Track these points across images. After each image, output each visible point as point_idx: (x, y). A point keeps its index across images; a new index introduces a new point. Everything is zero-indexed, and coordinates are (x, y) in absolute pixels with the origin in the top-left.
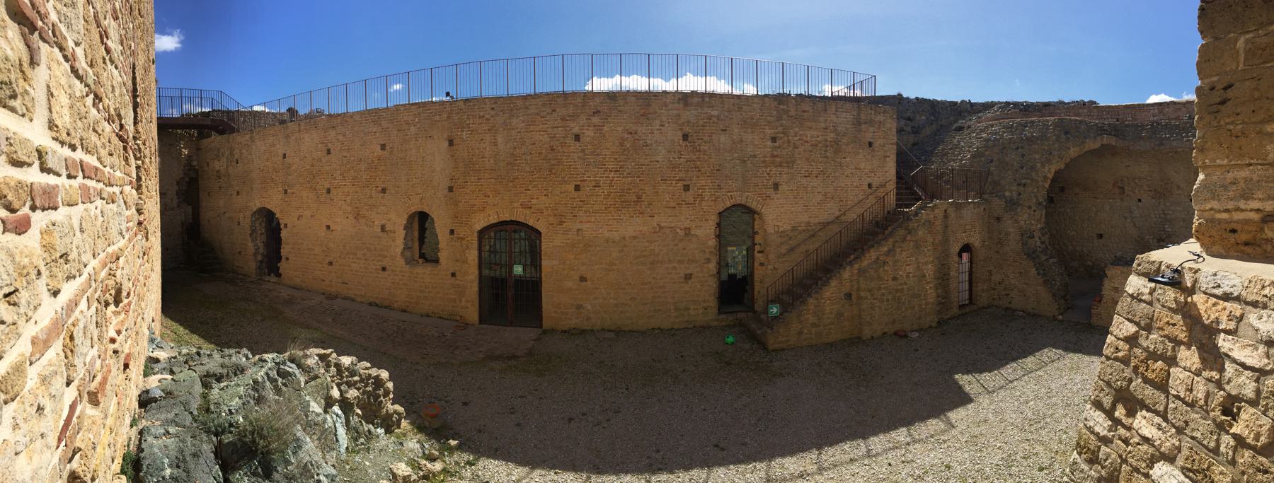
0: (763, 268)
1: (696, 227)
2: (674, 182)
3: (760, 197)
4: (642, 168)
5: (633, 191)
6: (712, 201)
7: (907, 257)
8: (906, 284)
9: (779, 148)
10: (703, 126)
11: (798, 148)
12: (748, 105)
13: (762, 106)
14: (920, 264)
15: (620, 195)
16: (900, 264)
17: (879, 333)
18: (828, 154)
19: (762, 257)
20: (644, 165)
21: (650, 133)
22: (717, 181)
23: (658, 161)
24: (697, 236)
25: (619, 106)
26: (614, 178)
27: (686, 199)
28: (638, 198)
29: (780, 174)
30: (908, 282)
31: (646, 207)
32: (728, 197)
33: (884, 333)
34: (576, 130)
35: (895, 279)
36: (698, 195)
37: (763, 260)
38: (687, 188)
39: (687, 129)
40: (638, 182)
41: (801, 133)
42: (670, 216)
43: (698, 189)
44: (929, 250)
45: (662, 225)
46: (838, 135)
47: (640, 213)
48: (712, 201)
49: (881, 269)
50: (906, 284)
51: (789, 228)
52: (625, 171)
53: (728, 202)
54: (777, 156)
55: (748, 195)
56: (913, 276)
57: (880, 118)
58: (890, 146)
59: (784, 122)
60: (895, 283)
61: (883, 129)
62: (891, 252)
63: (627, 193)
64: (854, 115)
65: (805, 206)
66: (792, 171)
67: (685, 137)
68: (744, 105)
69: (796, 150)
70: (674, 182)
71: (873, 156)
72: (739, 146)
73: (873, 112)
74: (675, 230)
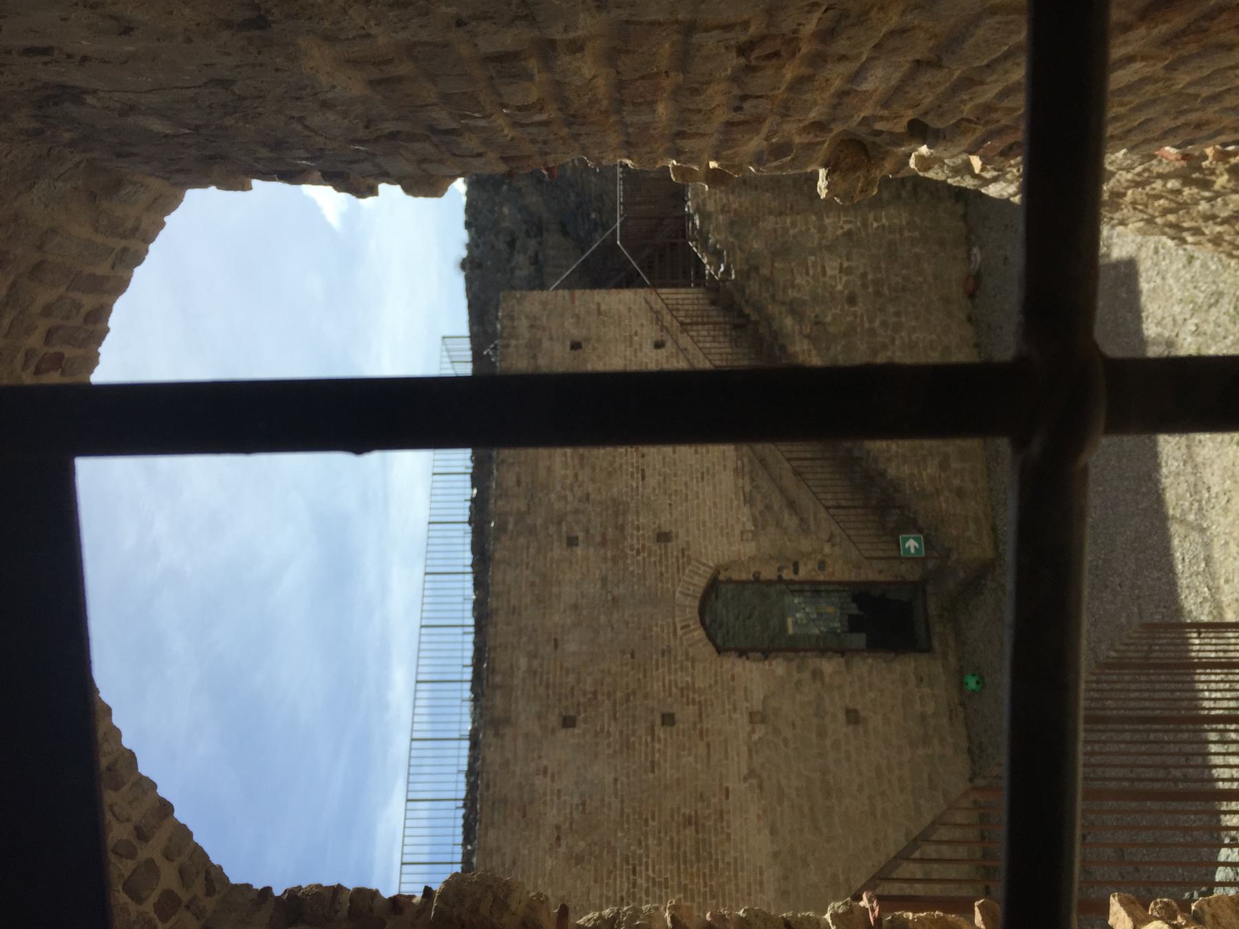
0: (829, 561)
1: (747, 700)
3: (684, 569)
4: (628, 815)
5: (674, 834)
7: (807, 273)
8: (864, 275)
9: (587, 531)
10: (547, 687)
11: (588, 495)
12: (509, 592)
14: (824, 242)
15: (685, 862)
16: (820, 290)
19: (806, 564)
20: (622, 809)
21: (559, 798)
22: (655, 657)
23: (616, 780)
25: (503, 865)
26: (648, 877)
27: (691, 720)
28: (690, 824)
29: (638, 529)
30: (861, 270)
31: (708, 807)
32: (685, 634)
33: (969, 319)
35: (852, 300)
36: (682, 695)
37: (812, 565)
38: (668, 719)
39: (554, 720)
40: (655, 823)
41: (559, 488)
42: (726, 752)
43: (670, 695)
45: (745, 770)
47: (722, 818)
49: (832, 330)
50: (864, 275)
51: (746, 510)
52: (634, 853)
53: (696, 634)
54: (604, 536)
55: (681, 593)
56: (848, 259)
57: (523, 325)
58: (577, 303)
59: (539, 521)
60: (860, 299)
61: (544, 319)
62: (795, 309)
63: (679, 848)
65: (702, 478)
66: (632, 505)
67: (568, 722)
68: (509, 601)
69: (592, 497)
70: (657, 746)
71: (599, 340)
72: (585, 613)
73: (513, 342)
74: (755, 743)
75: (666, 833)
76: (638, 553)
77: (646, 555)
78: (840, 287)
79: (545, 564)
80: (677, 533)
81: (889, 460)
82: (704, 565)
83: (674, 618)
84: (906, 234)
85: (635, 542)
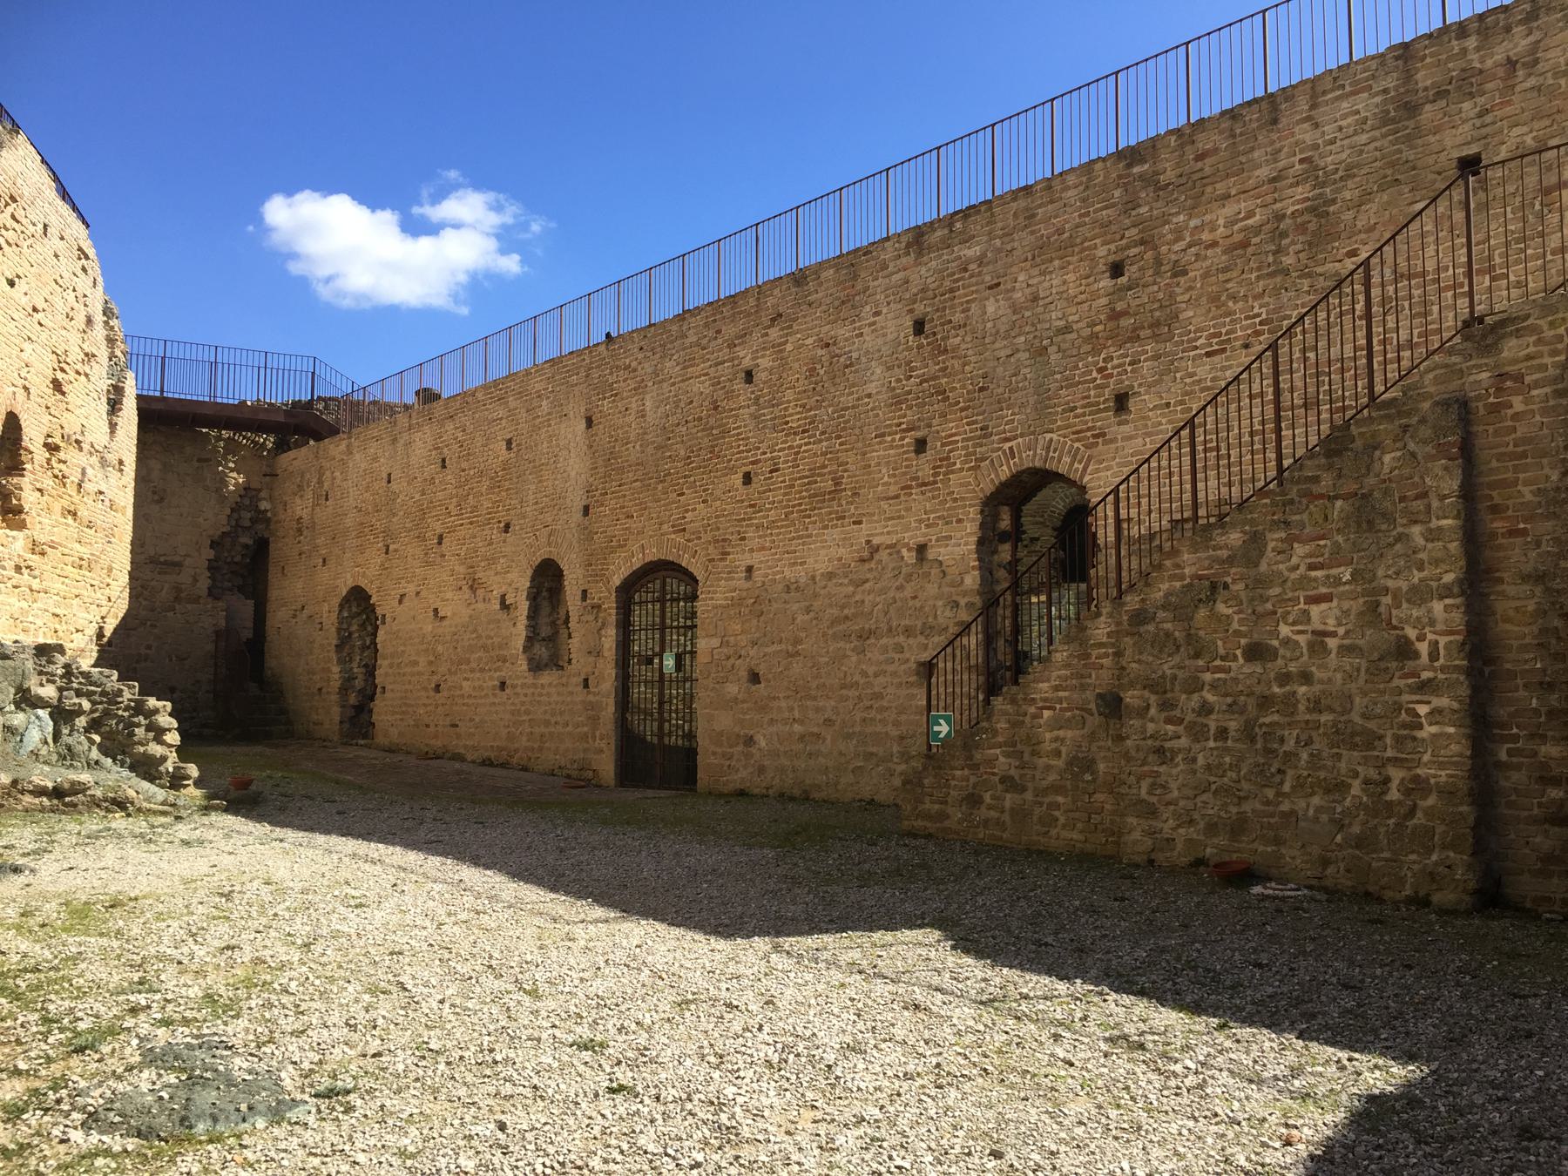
2: (898, 437)
3: (1078, 440)
4: (843, 416)
6: (970, 469)
7: (1312, 567)
8: (1306, 677)
9: (1130, 289)
10: (952, 290)
11: (1185, 273)
14: (1387, 600)
16: (1276, 591)
17: (1179, 855)
18: (1288, 260)
20: (848, 408)
23: (869, 396)
24: (941, 563)
26: (800, 446)
30: (1318, 674)
34: (747, 363)
35: (1256, 652)
36: (941, 460)
38: (921, 446)
39: (920, 308)
43: (943, 445)
44: (1432, 535)
45: (876, 541)
46: (1323, 185)
48: (970, 469)
49: (1202, 612)
50: (1306, 677)
53: (1005, 468)
54: (1125, 313)
55: (1051, 440)
56: (1344, 650)
64: (1385, 91)
67: (919, 327)
69: (1182, 280)
70: (898, 437)
72: (1027, 314)
74: (899, 552)
75: (829, 460)
76: (1100, 370)
77: (1098, 382)
78: (1285, 630)
79: (1086, 240)
80: (1126, 422)
81: (1013, 701)
82: (1085, 469)
83: (1022, 435)
84: (1397, 775)
85: (1116, 362)
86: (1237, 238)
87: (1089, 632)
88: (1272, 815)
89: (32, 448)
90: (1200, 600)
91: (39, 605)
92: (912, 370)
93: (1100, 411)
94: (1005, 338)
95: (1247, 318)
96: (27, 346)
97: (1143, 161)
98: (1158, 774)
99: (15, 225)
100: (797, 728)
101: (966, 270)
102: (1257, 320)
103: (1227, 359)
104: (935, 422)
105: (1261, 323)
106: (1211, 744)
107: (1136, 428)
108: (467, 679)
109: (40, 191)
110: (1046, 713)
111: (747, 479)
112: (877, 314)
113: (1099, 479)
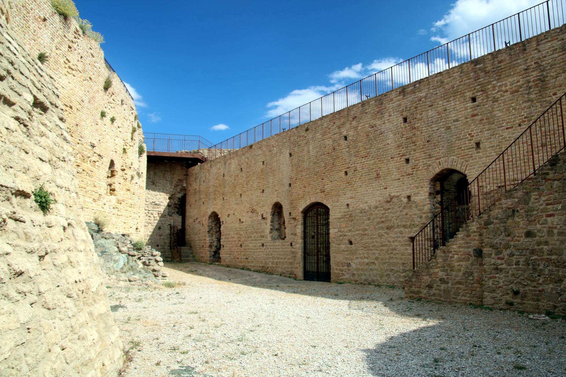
2: (399, 158)
3: (463, 159)
6: (425, 169)
7: (547, 204)
9: (478, 106)
10: (416, 108)
11: (497, 101)
13: (461, 73)
16: (535, 212)
18: (533, 96)
22: (428, 151)
23: (388, 144)
26: (364, 162)
34: (345, 133)
35: (529, 234)
36: (415, 166)
38: (407, 161)
39: (405, 114)
46: (542, 71)
48: (425, 169)
49: (510, 220)
50: (546, 243)
54: (476, 115)
55: (453, 159)
60: (530, 239)
66: (493, 126)
67: (405, 120)
72: (443, 115)
76: (470, 134)
77: (469, 138)
81: (444, 252)
82: (466, 168)
83: (443, 157)
85: (475, 131)
86: (514, 89)
87: (470, 228)
88: (536, 291)
89: (117, 170)
90: (509, 216)
91: (120, 220)
92: (403, 135)
93: (470, 148)
94: (436, 124)
95: (520, 116)
96: (117, 139)
97: (479, 64)
98: (495, 277)
99: (113, 102)
100: (366, 260)
101: (420, 101)
102: (523, 117)
103: (514, 130)
104: (412, 153)
105: (525, 118)
106: (514, 266)
107: (483, 154)
108: (250, 243)
109: (120, 91)
110: (456, 256)
111: (346, 173)
112: (390, 116)
113: (471, 172)
